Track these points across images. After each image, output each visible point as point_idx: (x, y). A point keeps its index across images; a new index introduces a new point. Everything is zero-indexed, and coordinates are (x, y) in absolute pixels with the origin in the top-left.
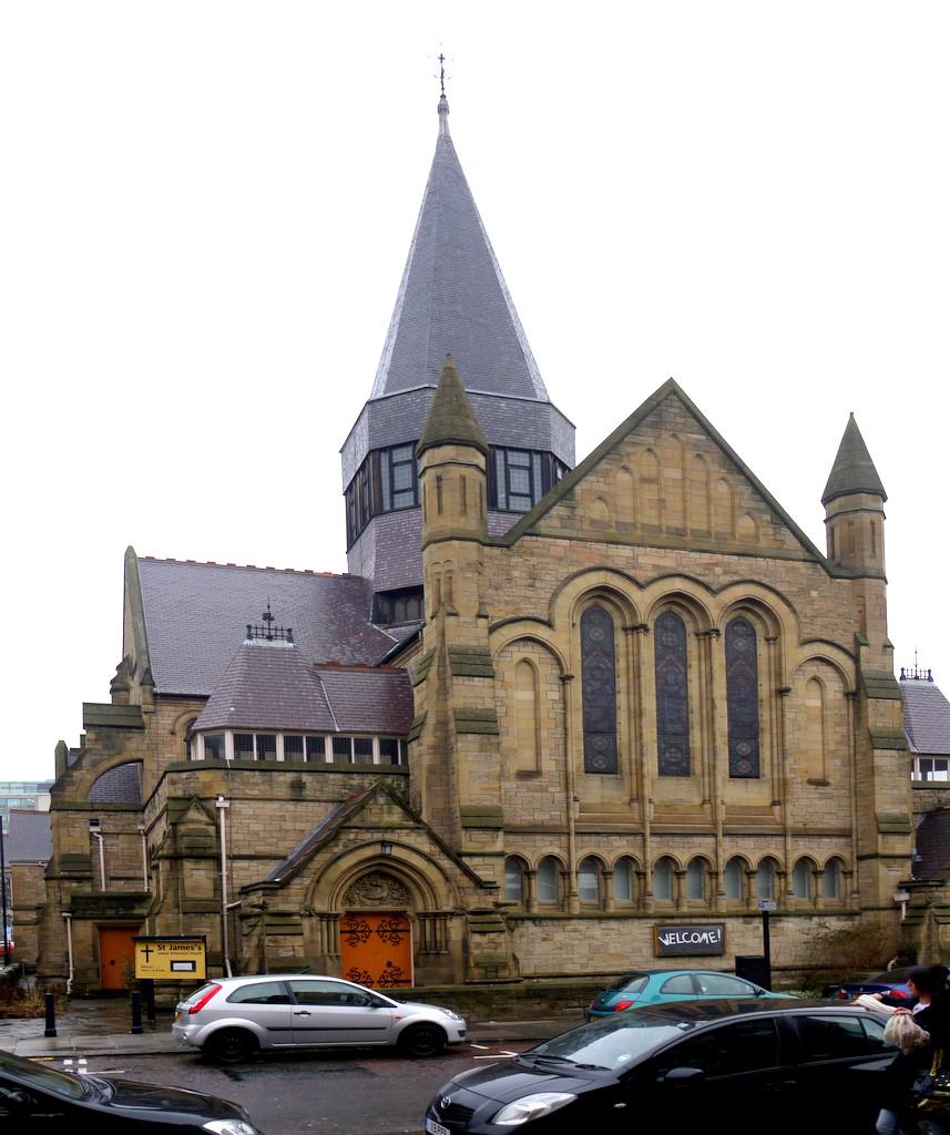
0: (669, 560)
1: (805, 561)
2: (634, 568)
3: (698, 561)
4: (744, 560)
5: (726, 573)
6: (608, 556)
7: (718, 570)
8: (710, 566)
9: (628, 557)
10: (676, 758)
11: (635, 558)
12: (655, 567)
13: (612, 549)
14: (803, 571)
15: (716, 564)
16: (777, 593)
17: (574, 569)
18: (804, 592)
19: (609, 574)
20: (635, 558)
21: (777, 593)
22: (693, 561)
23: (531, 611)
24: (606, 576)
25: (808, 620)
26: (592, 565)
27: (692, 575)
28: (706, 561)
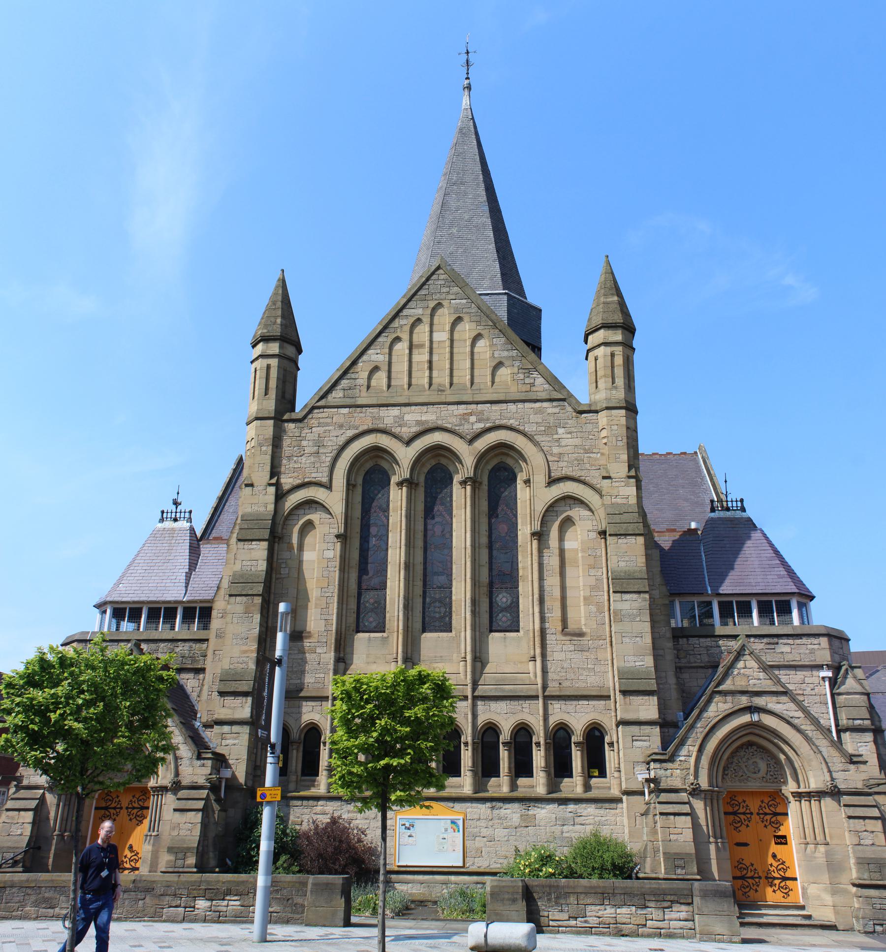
0: (430, 416)
1: (551, 400)
2: (400, 426)
3: (456, 412)
4: (495, 407)
5: (479, 421)
6: (379, 418)
7: (473, 419)
8: (465, 417)
9: (394, 417)
10: (440, 613)
11: (401, 417)
12: (418, 423)
13: (383, 412)
14: (550, 411)
15: (471, 414)
16: (525, 434)
17: (350, 433)
18: (550, 430)
19: (379, 435)
20: (401, 417)
21: (525, 434)
22: (450, 415)
23: (314, 475)
24: (376, 437)
25: (556, 459)
26: (365, 427)
27: (449, 426)
28: (461, 412)
